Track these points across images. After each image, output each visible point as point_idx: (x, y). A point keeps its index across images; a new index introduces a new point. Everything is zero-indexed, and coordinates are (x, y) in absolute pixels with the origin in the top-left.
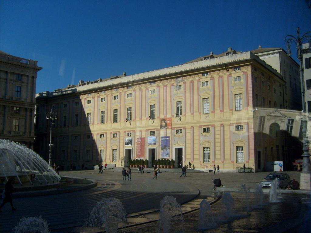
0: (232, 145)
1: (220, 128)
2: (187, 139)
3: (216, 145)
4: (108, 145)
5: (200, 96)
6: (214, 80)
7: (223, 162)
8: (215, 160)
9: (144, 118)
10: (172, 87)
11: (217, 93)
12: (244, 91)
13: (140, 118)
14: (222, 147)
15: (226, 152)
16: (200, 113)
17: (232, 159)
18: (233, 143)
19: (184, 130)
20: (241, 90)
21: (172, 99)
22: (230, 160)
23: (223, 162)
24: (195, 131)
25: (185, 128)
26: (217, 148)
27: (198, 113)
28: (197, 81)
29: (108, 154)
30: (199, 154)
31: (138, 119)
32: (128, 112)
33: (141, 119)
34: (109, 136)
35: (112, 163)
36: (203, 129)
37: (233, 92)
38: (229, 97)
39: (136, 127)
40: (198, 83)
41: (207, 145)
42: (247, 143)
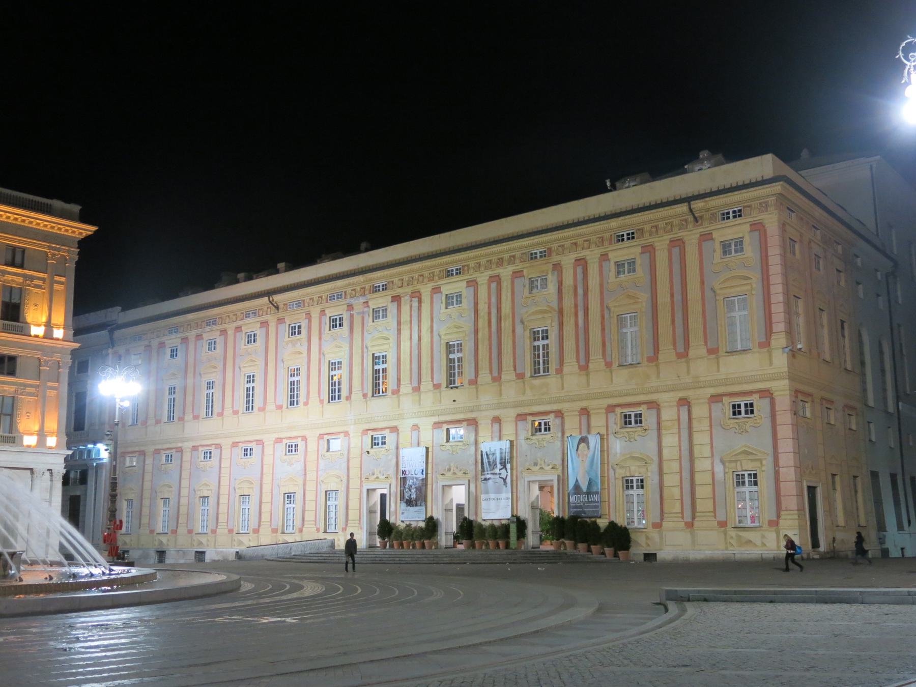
0: (719, 468)
1: (679, 410)
3: (665, 470)
4: (311, 476)
7: (690, 525)
8: (662, 519)
9: (426, 385)
10: (516, 281)
11: (663, 298)
12: (754, 286)
13: (415, 384)
14: (686, 475)
15: (700, 492)
16: (609, 365)
17: (721, 517)
18: (723, 462)
19: (558, 421)
20: (745, 282)
21: (517, 321)
22: (715, 517)
23: (690, 525)
24: (593, 423)
25: (559, 414)
28: (597, 260)
29: (310, 506)
31: (406, 388)
33: (417, 389)
35: (322, 536)
36: (619, 415)
37: (718, 292)
38: (703, 305)
39: (401, 417)
40: (601, 266)
42: (768, 463)
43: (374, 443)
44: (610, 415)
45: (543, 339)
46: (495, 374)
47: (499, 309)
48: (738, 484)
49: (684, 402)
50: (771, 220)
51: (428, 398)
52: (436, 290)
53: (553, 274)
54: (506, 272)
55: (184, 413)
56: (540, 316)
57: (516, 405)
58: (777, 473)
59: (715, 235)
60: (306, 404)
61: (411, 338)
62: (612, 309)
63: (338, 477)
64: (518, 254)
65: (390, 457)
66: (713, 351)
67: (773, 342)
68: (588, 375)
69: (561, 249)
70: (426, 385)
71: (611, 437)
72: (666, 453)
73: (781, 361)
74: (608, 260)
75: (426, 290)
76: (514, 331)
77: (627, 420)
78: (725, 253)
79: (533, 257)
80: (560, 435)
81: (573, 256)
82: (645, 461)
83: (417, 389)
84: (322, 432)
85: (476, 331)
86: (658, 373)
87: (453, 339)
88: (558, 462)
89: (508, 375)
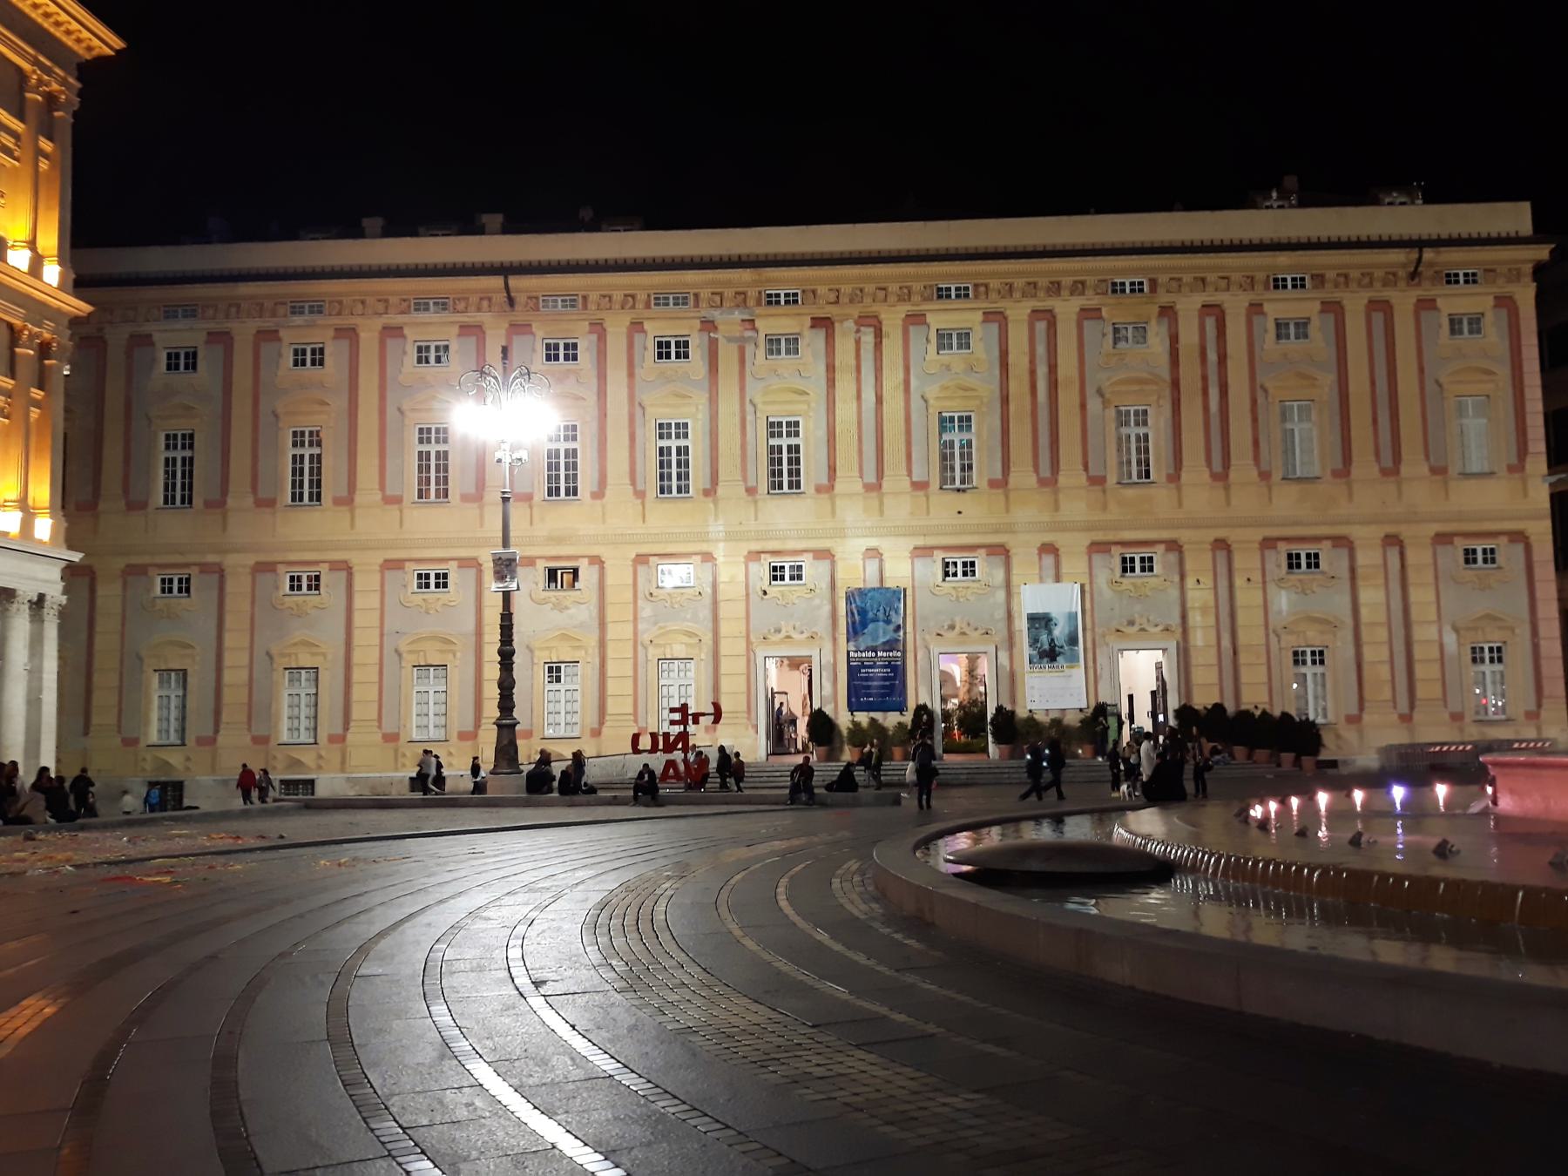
0: (1450, 639)
2: (1189, 604)
5: (1266, 391)
6: (1343, 314)
8: (1361, 708)
9: (896, 480)
10: (1086, 323)
13: (871, 478)
15: (1420, 671)
16: (1265, 476)
17: (1454, 706)
18: (1456, 630)
19: (1173, 557)
20: (1485, 377)
23: (1406, 718)
26: (1368, 654)
27: (1254, 473)
30: (1270, 679)
31: (848, 482)
32: (946, 437)
33: (875, 487)
34: (619, 575)
39: (841, 534)
41: (1313, 638)
42: (1524, 631)
43: (776, 574)
44: (1267, 553)
45: (1137, 424)
46: (1046, 472)
47: (1053, 368)
48: (1474, 660)
49: (1392, 541)
50: (1526, 295)
51: (900, 505)
52: (916, 319)
53: (1159, 323)
54: (1067, 308)
55: (225, 492)
56: (1136, 388)
57: (1089, 528)
58: (1536, 647)
59: (1440, 302)
60: (599, 494)
61: (859, 397)
62: (1271, 391)
63: (690, 634)
64: (1091, 280)
65: (817, 601)
66: (1439, 471)
67: (1528, 466)
68: (1227, 488)
69: (1174, 284)
70: (896, 480)
71: (1271, 588)
72: (1364, 612)
73: (1540, 495)
74: (1263, 313)
75: (892, 318)
76: (1083, 406)
77: (1293, 562)
78: (1453, 332)
79: (1117, 289)
80: (1177, 579)
81: (1199, 299)
82: (1330, 625)
83: (875, 487)
84: (645, 549)
85: (1005, 400)
86: (1350, 495)
87: (955, 409)
88: (1175, 620)
89: (1073, 476)
